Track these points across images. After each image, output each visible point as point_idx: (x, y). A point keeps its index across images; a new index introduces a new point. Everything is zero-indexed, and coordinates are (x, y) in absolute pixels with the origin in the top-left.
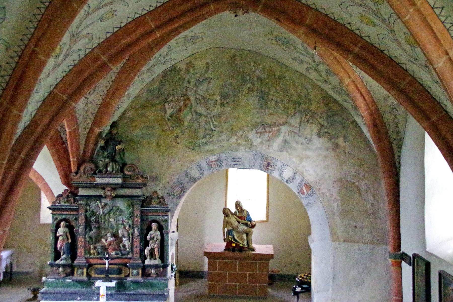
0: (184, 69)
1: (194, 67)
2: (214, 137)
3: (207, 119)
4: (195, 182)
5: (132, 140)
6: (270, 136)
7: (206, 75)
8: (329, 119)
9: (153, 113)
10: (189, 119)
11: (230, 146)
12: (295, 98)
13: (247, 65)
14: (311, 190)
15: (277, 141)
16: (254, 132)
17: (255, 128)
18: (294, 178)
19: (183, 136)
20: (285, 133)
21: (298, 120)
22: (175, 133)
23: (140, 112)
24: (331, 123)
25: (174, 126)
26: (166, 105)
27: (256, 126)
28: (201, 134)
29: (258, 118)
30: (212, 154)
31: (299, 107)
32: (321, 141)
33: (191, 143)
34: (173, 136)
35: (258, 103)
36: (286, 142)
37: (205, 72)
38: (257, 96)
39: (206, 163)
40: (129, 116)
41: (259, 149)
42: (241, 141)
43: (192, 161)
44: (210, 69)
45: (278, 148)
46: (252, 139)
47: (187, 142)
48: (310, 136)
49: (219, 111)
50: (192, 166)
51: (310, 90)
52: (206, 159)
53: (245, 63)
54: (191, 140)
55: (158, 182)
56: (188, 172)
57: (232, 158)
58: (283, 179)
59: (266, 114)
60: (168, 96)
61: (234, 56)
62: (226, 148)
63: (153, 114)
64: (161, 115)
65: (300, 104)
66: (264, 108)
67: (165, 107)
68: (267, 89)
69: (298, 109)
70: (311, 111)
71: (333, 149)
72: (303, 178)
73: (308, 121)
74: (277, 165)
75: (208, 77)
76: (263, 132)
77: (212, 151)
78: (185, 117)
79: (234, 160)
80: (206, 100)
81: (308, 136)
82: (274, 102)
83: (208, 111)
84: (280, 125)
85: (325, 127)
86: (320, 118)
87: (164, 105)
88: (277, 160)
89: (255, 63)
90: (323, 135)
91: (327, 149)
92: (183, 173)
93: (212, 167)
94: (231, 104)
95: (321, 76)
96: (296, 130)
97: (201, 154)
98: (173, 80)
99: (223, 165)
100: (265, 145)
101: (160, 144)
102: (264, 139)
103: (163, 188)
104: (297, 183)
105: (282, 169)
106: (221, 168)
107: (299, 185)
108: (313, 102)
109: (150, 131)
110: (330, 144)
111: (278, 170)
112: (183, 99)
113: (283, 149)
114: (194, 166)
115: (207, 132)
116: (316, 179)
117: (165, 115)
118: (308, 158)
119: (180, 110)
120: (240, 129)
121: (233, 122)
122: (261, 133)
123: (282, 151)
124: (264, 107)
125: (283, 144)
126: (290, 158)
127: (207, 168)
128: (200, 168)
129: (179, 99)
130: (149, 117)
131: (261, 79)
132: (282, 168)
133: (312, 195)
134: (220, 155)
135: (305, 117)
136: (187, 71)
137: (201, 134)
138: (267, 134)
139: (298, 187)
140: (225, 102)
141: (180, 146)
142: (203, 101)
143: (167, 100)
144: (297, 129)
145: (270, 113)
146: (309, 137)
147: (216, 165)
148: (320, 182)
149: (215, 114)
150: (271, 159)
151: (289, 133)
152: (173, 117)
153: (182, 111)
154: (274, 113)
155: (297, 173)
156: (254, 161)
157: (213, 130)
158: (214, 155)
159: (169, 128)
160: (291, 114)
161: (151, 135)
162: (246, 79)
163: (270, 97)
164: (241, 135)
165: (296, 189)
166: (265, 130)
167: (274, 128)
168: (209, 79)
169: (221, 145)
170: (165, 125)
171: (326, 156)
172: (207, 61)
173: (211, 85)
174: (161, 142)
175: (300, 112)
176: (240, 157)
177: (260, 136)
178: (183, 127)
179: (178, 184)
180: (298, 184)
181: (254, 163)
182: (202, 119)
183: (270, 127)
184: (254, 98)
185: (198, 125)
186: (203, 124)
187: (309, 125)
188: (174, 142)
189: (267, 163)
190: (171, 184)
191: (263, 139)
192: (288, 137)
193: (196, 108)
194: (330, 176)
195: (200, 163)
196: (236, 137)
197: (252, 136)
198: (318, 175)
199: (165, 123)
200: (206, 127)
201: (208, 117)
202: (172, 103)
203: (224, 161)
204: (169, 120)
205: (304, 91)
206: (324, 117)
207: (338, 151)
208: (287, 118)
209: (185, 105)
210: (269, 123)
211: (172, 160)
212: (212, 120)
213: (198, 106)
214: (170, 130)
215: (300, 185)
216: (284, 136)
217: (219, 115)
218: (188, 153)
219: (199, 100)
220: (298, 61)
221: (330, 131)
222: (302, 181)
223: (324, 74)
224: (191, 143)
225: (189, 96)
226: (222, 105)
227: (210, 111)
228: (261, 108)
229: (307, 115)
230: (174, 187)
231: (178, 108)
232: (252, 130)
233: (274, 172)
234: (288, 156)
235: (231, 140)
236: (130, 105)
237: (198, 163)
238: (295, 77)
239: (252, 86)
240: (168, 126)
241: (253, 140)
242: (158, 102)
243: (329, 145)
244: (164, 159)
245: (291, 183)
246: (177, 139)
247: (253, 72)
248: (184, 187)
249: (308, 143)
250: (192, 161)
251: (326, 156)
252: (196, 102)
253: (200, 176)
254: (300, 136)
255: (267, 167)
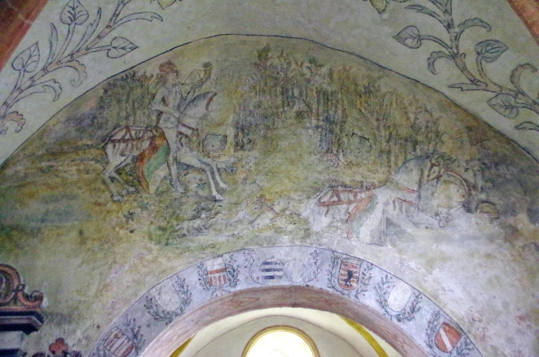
0: (155, 76)
1: (177, 72)
2: (220, 215)
3: (204, 177)
4: (167, 324)
5: (16, 228)
6: (350, 210)
7: (204, 87)
8: (487, 173)
9: (75, 165)
10: (162, 176)
11: (257, 234)
12: (404, 132)
13: (294, 66)
14: (462, 339)
15: (368, 222)
16: (313, 202)
17: (314, 194)
18: (416, 310)
19: (145, 214)
20: (386, 204)
21: (415, 175)
22: (126, 208)
23: (44, 164)
24: (492, 182)
25: (124, 192)
26: (110, 148)
27: (317, 190)
28: (188, 210)
29: (320, 173)
30: (213, 253)
31: (415, 150)
32: (474, 220)
33: (164, 229)
34: (120, 214)
35: (321, 141)
36: (389, 222)
37: (202, 82)
38: (317, 127)
39: (198, 275)
40: (17, 172)
41: (325, 241)
42: (281, 223)
43: (164, 271)
44: (213, 76)
45: (372, 236)
46: (308, 218)
47: (153, 227)
48: (445, 210)
49: (232, 160)
50: (162, 284)
51: (436, 114)
52: (198, 267)
53: (289, 64)
54: (163, 224)
55: (72, 327)
56: (151, 299)
57: (262, 261)
58: (389, 310)
59: (340, 163)
60: (115, 128)
61: (267, 50)
62: (246, 240)
63: (74, 168)
64: (95, 170)
65: (415, 143)
66: (335, 152)
67: (106, 153)
68: (340, 112)
69: (413, 153)
70: (442, 156)
71: (506, 240)
72: (437, 309)
73: (438, 178)
74: (370, 278)
75: (207, 90)
76: (334, 202)
77: (213, 246)
78: (152, 172)
79: (267, 267)
80: (203, 136)
81: (440, 209)
82: (356, 140)
83: (206, 160)
84: (374, 186)
85: (480, 189)
86: (466, 170)
87: (104, 148)
88: (372, 264)
89: (310, 62)
90: (477, 208)
91: (491, 239)
92: (138, 301)
93: (211, 285)
94: (260, 144)
95: (464, 69)
96: (412, 197)
97: (187, 254)
98: (128, 96)
99: (238, 280)
100: (339, 232)
101: (86, 234)
102: (338, 217)
103: (84, 342)
104: (425, 322)
105: (385, 286)
106: (236, 285)
107: (429, 326)
108: (445, 138)
109: (62, 206)
110: (497, 228)
111: (375, 288)
112: (150, 134)
113: (383, 240)
114: (169, 284)
115: (203, 205)
116: (471, 311)
117: (104, 169)
118: (445, 259)
119: (140, 158)
120: (281, 197)
121: (262, 181)
122: (328, 205)
123: (380, 244)
124: (334, 149)
125: (384, 227)
126: (401, 259)
127: (201, 288)
128: (183, 287)
129: (141, 135)
130: (66, 175)
131: (325, 93)
132: (383, 284)
133: (465, 351)
134: (234, 258)
135: (430, 169)
136: (162, 80)
137: (188, 210)
138: (345, 206)
139: (429, 332)
140: (245, 141)
141: (136, 237)
142: (194, 139)
143: (113, 139)
144: (415, 195)
145: (349, 161)
146: (443, 211)
147: (222, 279)
148: (484, 318)
149: (224, 166)
150: (355, 262)
151: (397, 204)
152: (124, 174)
153: (145, 160)
154: (360, 160)
155: (422, 296)
156: (314, 268)
157: (216, 201)
158: (219, 256)
159: (112, 196)
160: (396, 164)
161: (67, 214)
162: (293, 93)
163: (348, 128)
164: (284, 210)
165: (424, 335)
166: (338, 196)
167: (359, 195)
168: (210, 95)
169: (236, 232)
170: (103, 191)
171: (488, 256)
172: (205, 60)
173: (213, 106)
174: (90, 229)
175: (417, 158)
176: (280, 260)
177: (327, 211)
178: (144, 195)
179: (123, 328)
180: (427, 324)
181: (314, 273)
182: (193, 177)
183: (350, 191)
184: (310, 131)
185: (181, 190)
186: (193, 186)
187: (441, 187)
188: (122, 228)
189: (346, 273)
190: (105, 329)
191: (334, 218)
192: (393, 213)
193: (178, 155)
194: (506, 305)
195: (182, 275)
196: (270, 215)
197: (308, 211)
198: (475, 300)
199: (103, 187)
200: (201, 193)
201: (206, 172)
202: (125, 144)
203: (241, 270)
204: (112, 179)
205: (423, 118)
206: (476, 168)
207: (520, 243)
208: (389, 172)
209: (154, 148)
210: (348, 183)
211: (113, 270)
212: (214, 178)
213: (184, 149)
214: (114, 201)
215: (431, 325)
216: (384, 212)
217: (232, 167)
218: (155, 252)
219: (187, 136)
220: (409, 41)
221: (491, 199)
222: (437, 315)
223: (470, 61)
224: (164, 229)
225: (164, 130)
226: (239, 146)
227: (210, 159)
228: (329, 151)
229: (436, 166)
230: (112, 336)
231: (136, 153)
232: (309, 198)
233: (364, 295)
234: (398, 255)
235: (258, 221)
236: (23, 147)
237: (178, 277)
238: (402, 90)
239: (305, 109)
240: (110, 192)
241: (311, 220)
242: (89, 143)
243: (494, 229)
244: (93, 269)
245: (410, 320)
246: (130, 221)
247: (308, 81)
248: (139, 338)
249: (441, 225)
250: (164, 271)
251: (488, 256)
252: (180, 141)
253: (181, 308)
254: (423, 211)
255: (348, 283)
